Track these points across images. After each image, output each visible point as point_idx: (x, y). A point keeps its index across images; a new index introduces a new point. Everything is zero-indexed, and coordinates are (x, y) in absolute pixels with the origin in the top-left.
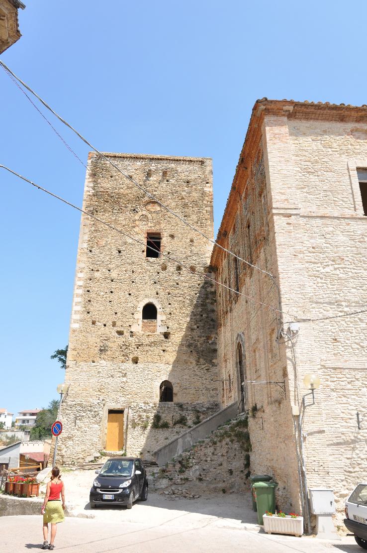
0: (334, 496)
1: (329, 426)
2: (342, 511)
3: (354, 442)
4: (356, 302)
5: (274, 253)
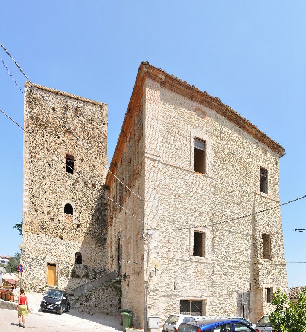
3: (171, 295)
4: (182, 223)
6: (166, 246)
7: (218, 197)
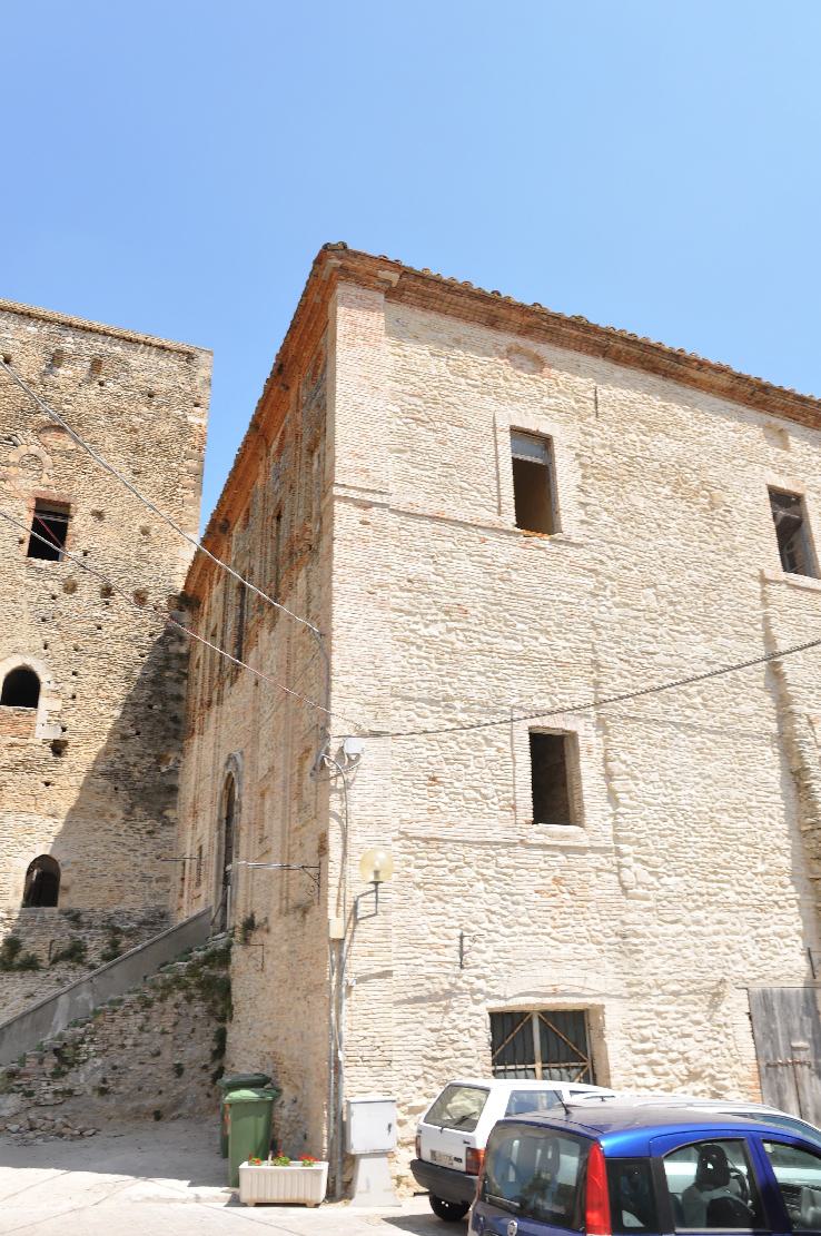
0: (398, 1111)
1: (403, 962)
2: (409, 1144)
3: (448, 994)
5: (326, 582)
6: (420, 792)
7: (609, 604)
